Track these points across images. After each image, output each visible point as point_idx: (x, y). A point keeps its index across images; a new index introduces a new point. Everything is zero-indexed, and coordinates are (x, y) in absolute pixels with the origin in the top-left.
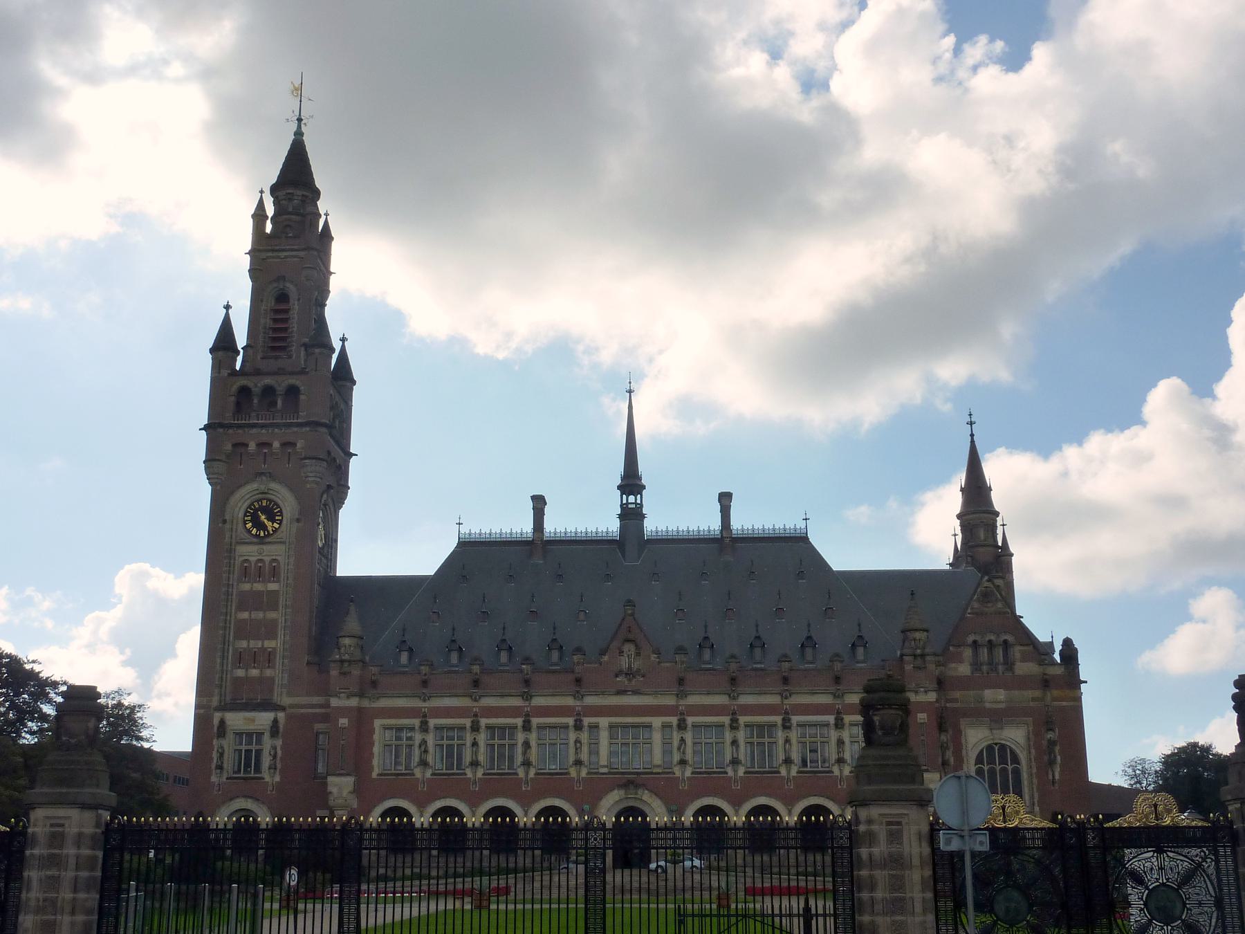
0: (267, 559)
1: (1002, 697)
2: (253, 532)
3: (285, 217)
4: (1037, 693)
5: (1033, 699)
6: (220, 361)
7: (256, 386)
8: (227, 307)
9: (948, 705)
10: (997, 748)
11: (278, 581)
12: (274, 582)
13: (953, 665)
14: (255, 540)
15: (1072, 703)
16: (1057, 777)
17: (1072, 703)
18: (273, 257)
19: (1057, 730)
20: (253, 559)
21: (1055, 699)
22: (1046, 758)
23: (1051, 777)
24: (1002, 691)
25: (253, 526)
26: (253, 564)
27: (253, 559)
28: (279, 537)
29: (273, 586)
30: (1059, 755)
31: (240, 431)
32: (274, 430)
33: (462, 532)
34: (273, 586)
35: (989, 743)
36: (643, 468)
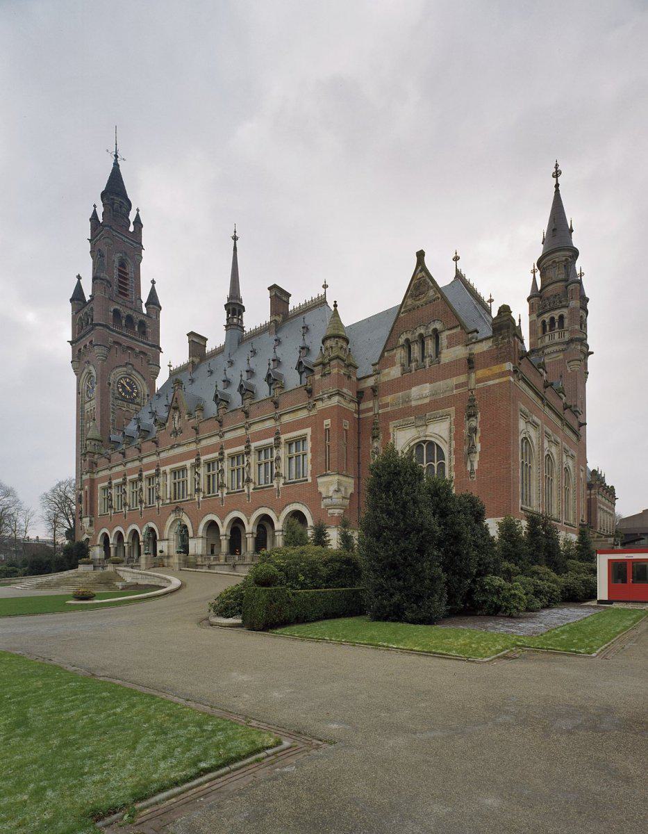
1: (428, 391)
4: (462, 379)
5: (457, 387)
8: (79, 277)
9: (380, 411)
10: (425, 446)
13: (387, 371)
15: (497, 381)
16: (476, 467)
17: (497, 381)
19: (479, 415)
21: (478, 381)
22: (466, 448)
23: (469, 469)
24: (428, 385)
30: (480, 441)
35: (418, 440)
36: (242, 294)
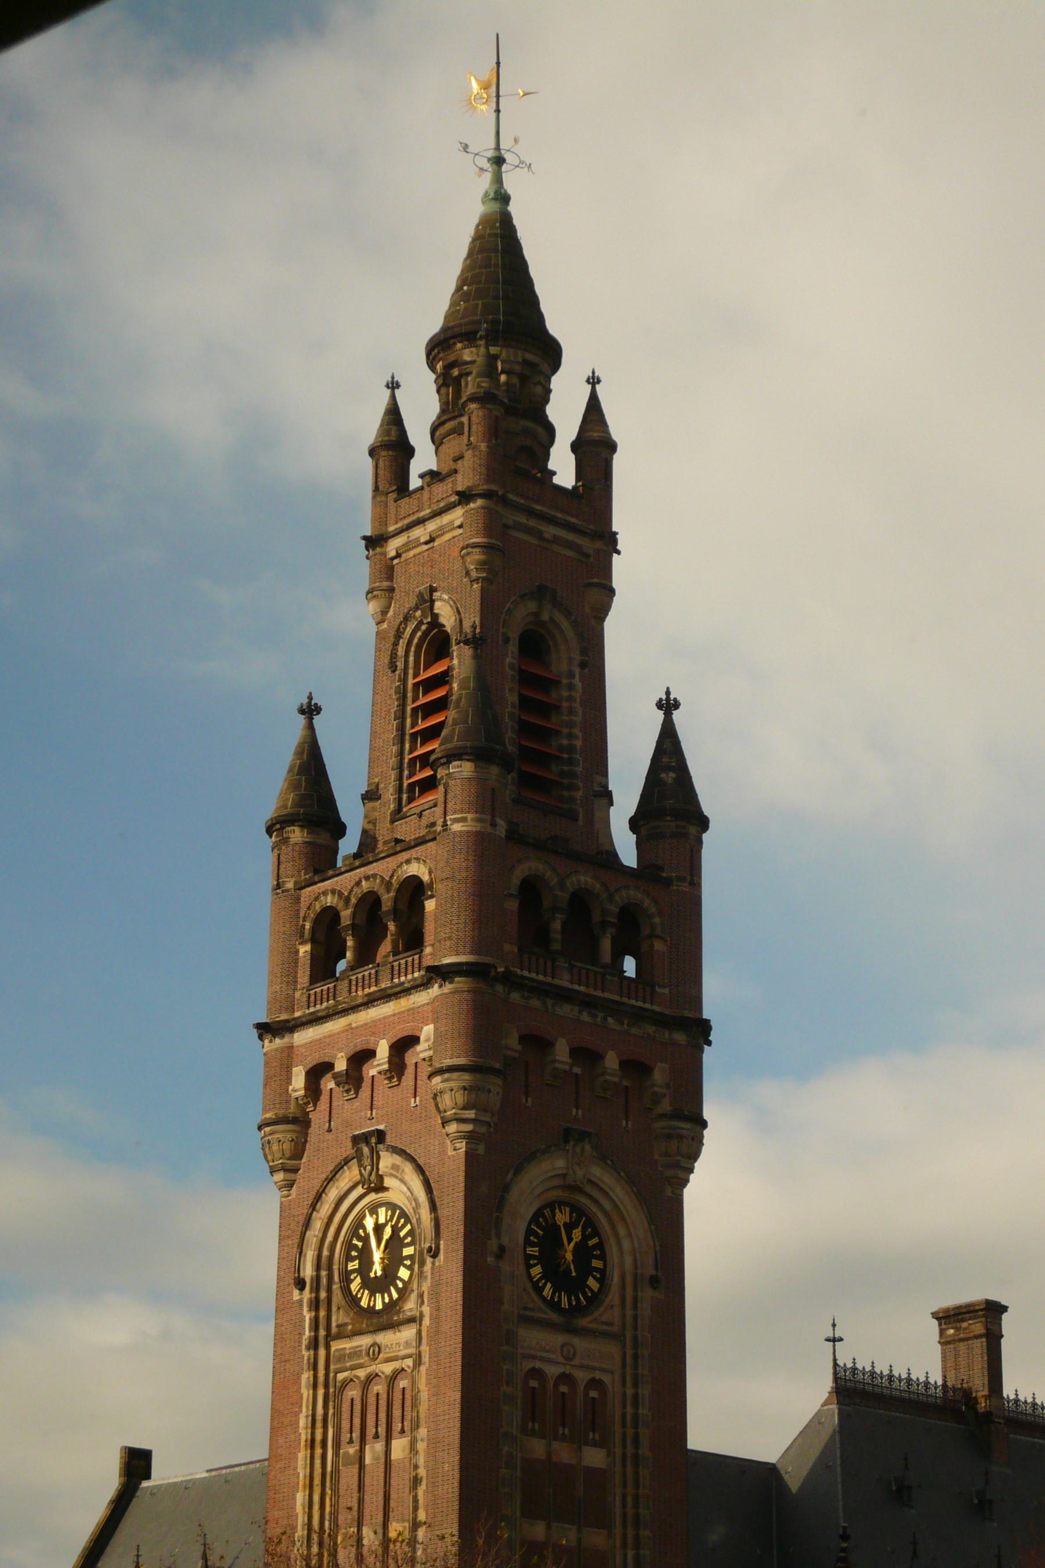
0: (582, 1377)
2: (545, 1293)
3: (523, 423)
6: (493, 790)
7: (562, 883)
11: (603, 1443)
12: (595, 1444)
14: (553, 1316)
18: (528, 530)
20: (552, 1371)
25: (546, 1276)
26: (551, 1384)
27: (552, 1371)
28: (605, 1318)
29: (594, 1457)
31: (535, 1003)
32: (605, 1018)
33: (840, 1362)
34: (594, 1457)
